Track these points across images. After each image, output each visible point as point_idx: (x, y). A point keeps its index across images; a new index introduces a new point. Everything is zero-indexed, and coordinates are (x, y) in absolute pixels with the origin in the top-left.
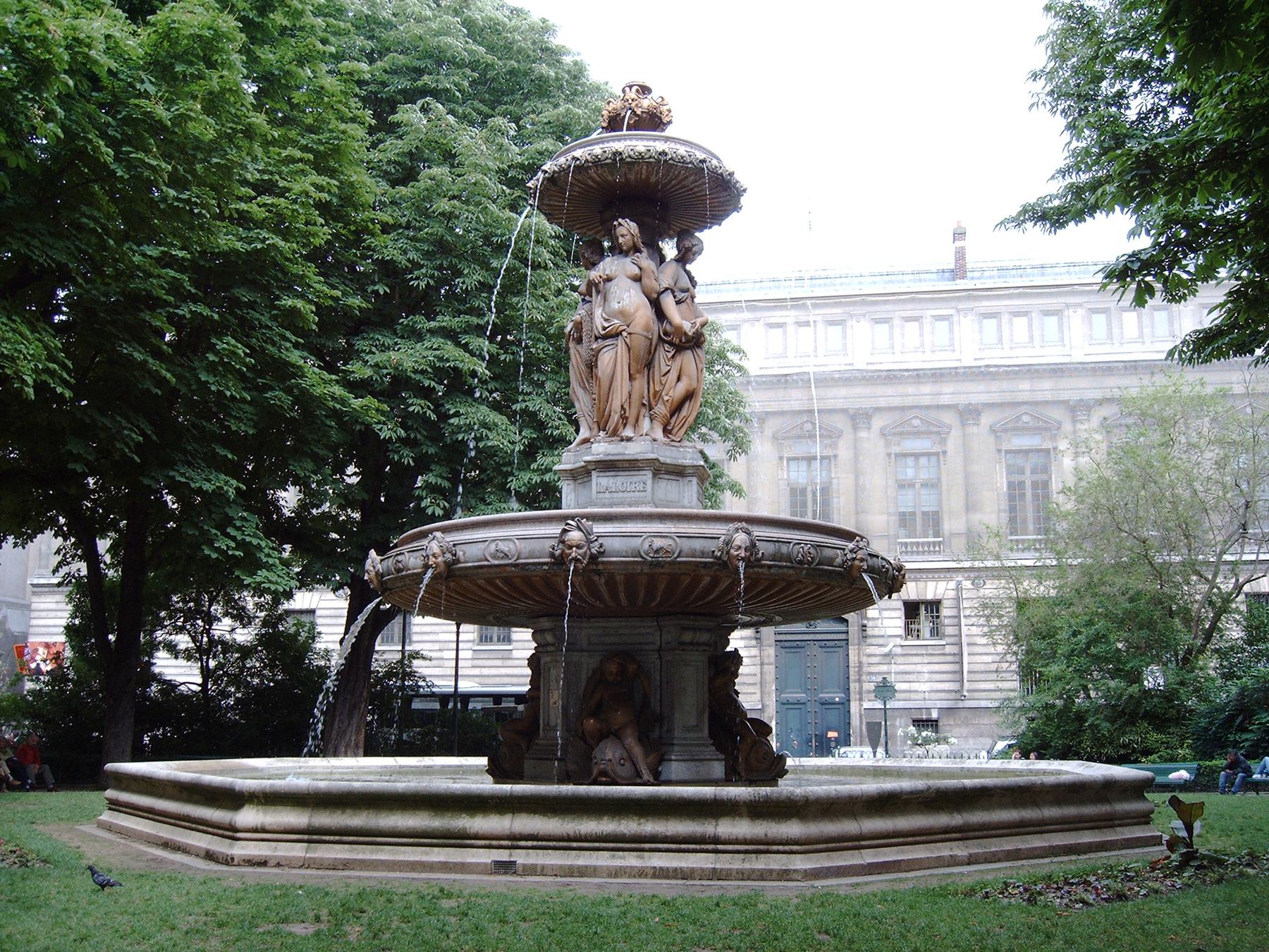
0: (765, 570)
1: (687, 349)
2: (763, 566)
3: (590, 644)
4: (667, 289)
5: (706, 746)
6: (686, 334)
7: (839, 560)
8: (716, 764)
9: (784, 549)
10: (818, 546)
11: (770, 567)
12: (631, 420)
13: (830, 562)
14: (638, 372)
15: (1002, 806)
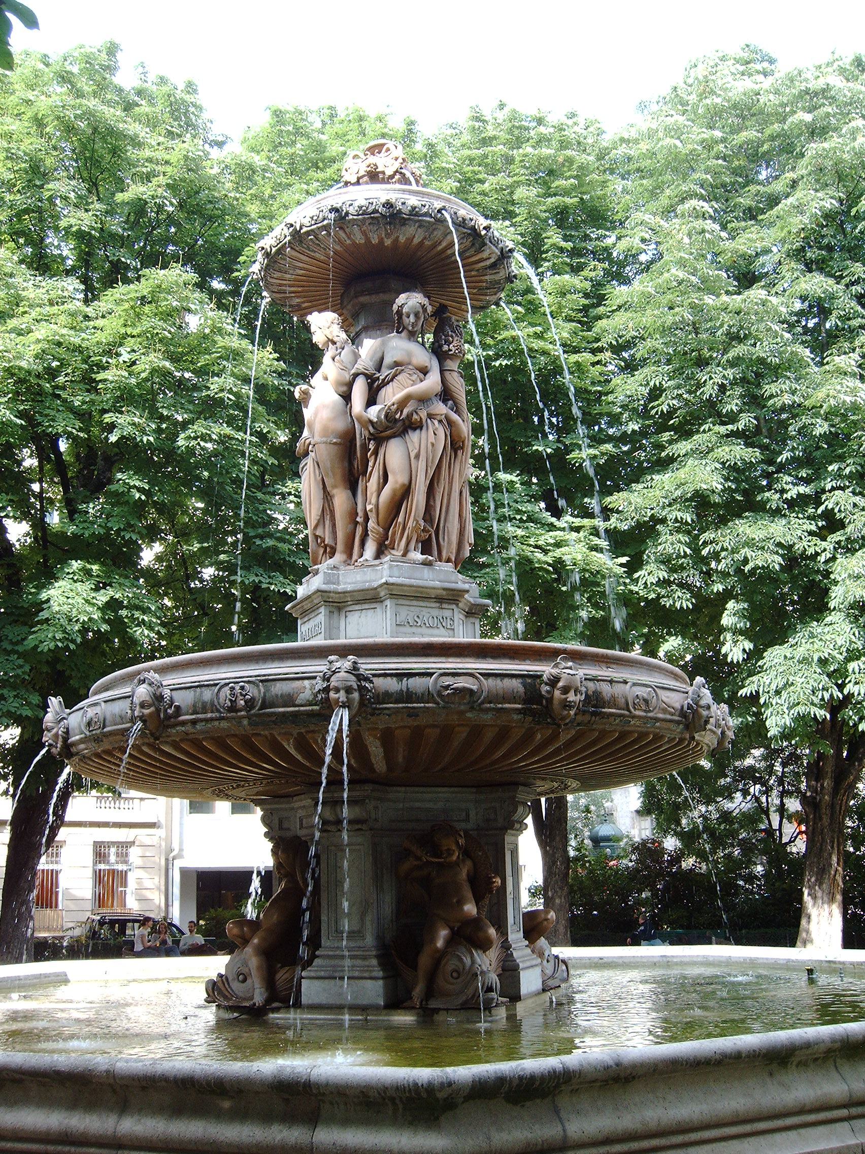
0: (189, 728)
1: (388, 438)
2: (184, 723)
3: (301, 827)
4: (356, 375)
5: (365, 958)
6: (371, 421)
7: (307, 695)
8: (369, 983)
9: (207, 695)
10: (266, 681)
11: (194, 722)
12: (340, 547)
13: (289, 700)
14: (335, 487)
15: (47, 1102)
